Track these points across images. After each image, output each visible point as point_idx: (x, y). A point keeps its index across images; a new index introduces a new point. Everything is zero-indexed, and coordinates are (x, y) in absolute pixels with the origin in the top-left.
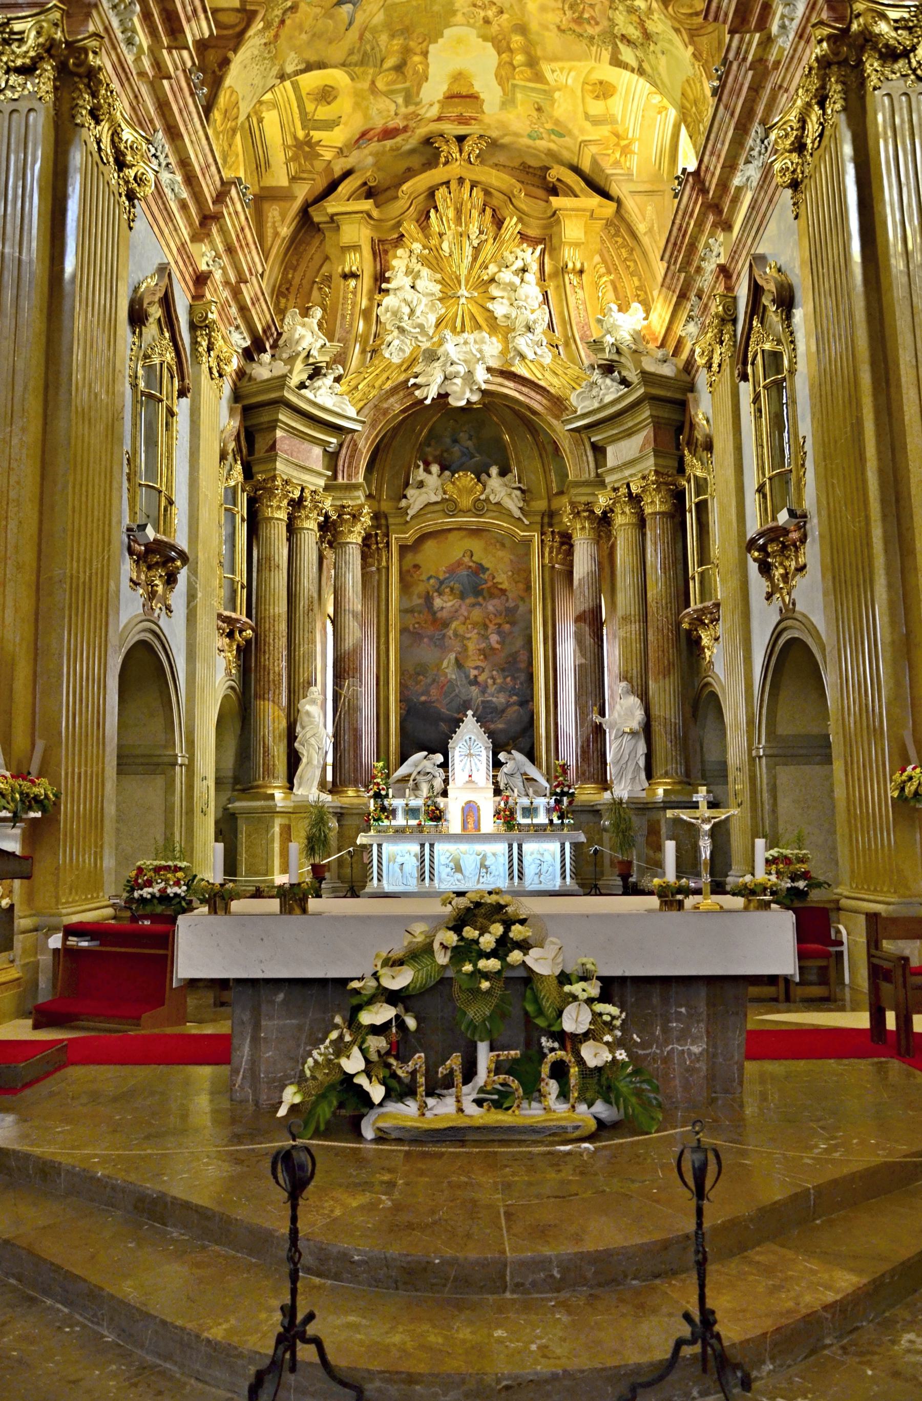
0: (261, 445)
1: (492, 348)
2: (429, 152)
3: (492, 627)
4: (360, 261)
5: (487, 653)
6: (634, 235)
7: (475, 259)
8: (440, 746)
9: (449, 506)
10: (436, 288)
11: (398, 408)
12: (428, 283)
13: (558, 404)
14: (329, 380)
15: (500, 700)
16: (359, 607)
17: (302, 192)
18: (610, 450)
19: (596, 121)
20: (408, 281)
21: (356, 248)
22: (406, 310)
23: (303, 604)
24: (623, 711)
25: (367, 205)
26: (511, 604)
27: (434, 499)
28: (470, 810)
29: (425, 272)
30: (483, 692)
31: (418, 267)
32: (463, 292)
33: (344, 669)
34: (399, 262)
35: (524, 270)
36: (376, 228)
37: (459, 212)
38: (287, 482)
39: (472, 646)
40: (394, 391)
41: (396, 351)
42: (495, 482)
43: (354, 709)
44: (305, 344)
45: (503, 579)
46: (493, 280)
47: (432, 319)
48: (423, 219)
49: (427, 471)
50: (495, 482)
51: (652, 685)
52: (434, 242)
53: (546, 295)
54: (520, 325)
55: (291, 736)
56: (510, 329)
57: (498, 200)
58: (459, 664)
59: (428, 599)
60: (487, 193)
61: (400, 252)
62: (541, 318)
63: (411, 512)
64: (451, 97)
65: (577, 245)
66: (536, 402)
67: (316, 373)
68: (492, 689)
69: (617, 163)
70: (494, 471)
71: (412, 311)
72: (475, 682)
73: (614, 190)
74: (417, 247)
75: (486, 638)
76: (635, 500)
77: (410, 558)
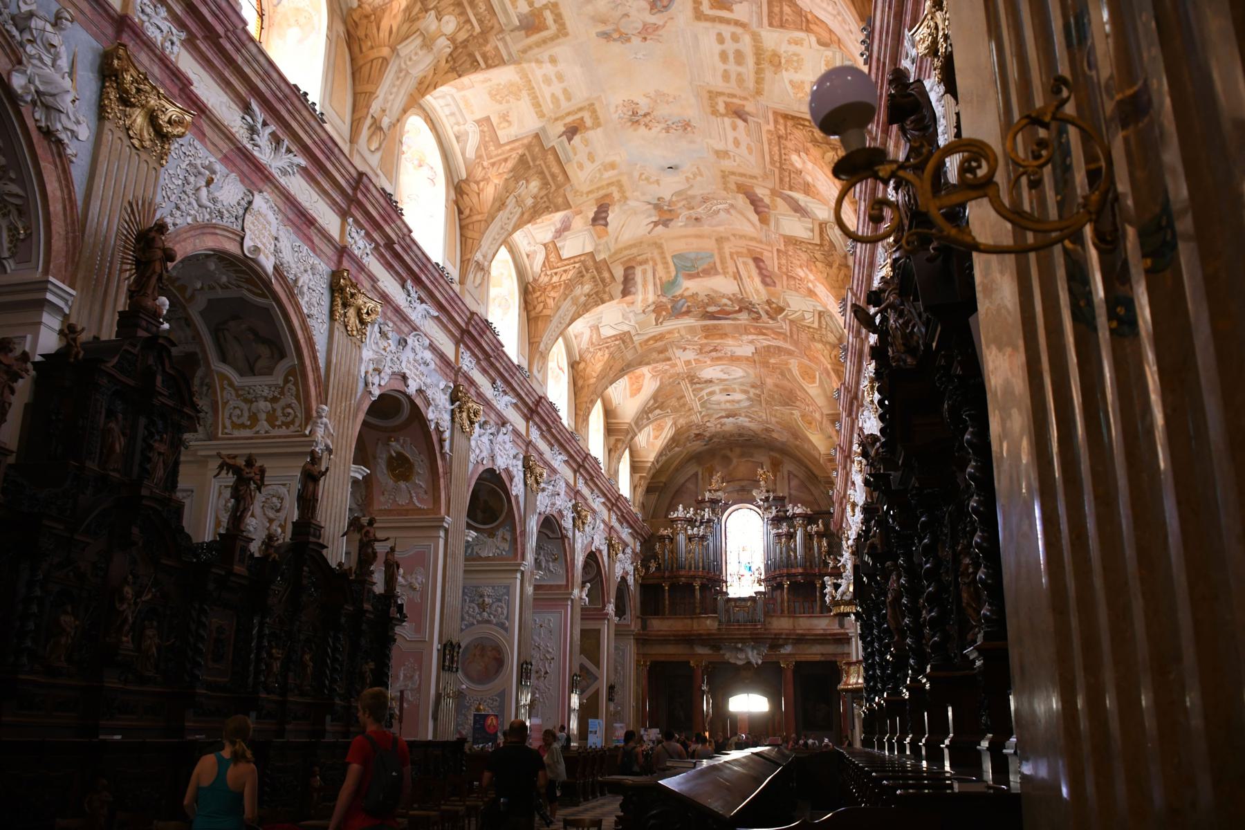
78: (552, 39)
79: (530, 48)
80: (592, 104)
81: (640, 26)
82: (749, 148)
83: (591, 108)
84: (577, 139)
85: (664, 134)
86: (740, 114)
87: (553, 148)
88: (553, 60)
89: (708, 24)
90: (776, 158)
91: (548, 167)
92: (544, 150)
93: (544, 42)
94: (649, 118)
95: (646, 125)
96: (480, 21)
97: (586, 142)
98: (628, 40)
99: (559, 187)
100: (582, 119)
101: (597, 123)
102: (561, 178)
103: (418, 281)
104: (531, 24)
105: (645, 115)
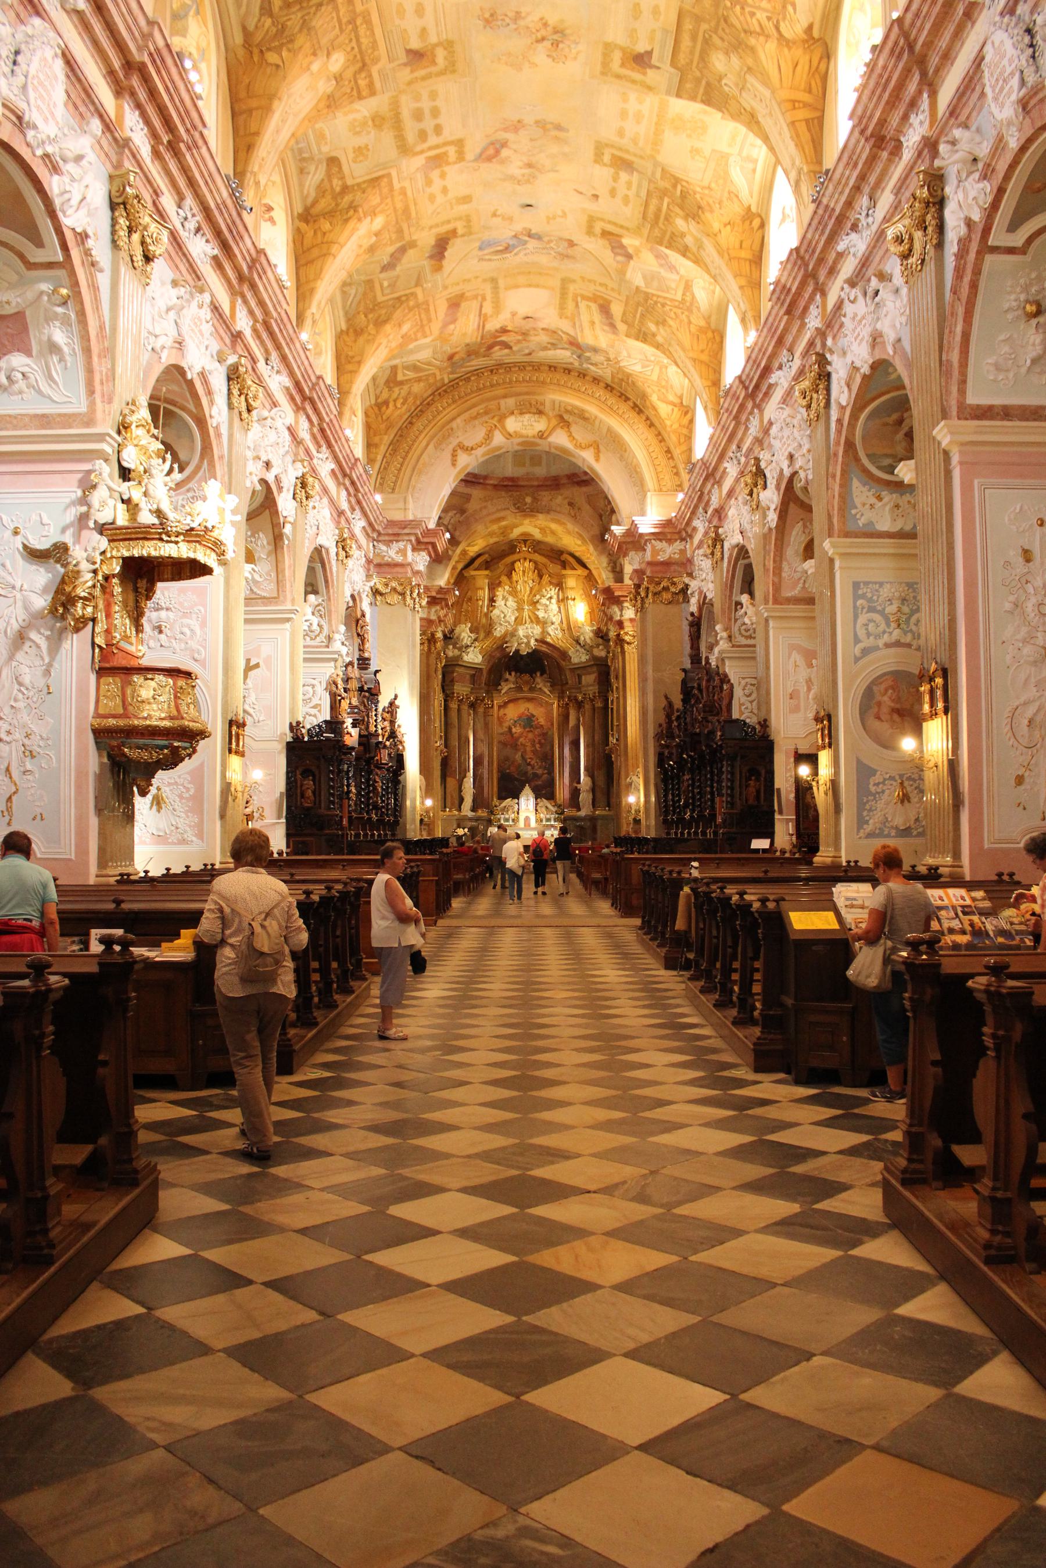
0: (448, 679)
1: (537, 630)
5: (534, 752)
8: (516, 796)
9: (519, 689)
10: (515, 605)
12: (511, 603)
13: (564, 655)
15: (540, 772)
21: (483, 589)
25: (487, 572)
28: (527, 819)
29: (510, 599)
34: (500, 593)
41: (498, 632)
43: (482, 778)
45: (542, 721)
48: (509, 576)
50: (538, 680)
55: (460, 791)
57: (540, 566)
59: (510, 729)
60: (536, 563)
62: (557, 620)
66: (555, 655)
67: (467, 647)
76: (592, 700)
77: (502, 712)
78: (612, 146)
79: (635, 155)
80: (603, 73)
81: (522, 132)
82: (401, 12)
83: (606, 70)
84: (641, 47)
85: (524, 10)
86: (416, 56)
87: (673, 63)
88: (621, 133)
89: (450, 139)
90: (362, 30)
91: (692, 53)
92: (683, 73)
93: (620, 149)
94: (539, 36)
95: (545, 25)
96: (661, 199)
97: (632, 33)
98: (537, 122)
99: (698, 19)
100: (623, 65)
101: (608, 48)
102: (688, 26)
103: (767, 371)
104: (623, 164)
105: (543, 39)
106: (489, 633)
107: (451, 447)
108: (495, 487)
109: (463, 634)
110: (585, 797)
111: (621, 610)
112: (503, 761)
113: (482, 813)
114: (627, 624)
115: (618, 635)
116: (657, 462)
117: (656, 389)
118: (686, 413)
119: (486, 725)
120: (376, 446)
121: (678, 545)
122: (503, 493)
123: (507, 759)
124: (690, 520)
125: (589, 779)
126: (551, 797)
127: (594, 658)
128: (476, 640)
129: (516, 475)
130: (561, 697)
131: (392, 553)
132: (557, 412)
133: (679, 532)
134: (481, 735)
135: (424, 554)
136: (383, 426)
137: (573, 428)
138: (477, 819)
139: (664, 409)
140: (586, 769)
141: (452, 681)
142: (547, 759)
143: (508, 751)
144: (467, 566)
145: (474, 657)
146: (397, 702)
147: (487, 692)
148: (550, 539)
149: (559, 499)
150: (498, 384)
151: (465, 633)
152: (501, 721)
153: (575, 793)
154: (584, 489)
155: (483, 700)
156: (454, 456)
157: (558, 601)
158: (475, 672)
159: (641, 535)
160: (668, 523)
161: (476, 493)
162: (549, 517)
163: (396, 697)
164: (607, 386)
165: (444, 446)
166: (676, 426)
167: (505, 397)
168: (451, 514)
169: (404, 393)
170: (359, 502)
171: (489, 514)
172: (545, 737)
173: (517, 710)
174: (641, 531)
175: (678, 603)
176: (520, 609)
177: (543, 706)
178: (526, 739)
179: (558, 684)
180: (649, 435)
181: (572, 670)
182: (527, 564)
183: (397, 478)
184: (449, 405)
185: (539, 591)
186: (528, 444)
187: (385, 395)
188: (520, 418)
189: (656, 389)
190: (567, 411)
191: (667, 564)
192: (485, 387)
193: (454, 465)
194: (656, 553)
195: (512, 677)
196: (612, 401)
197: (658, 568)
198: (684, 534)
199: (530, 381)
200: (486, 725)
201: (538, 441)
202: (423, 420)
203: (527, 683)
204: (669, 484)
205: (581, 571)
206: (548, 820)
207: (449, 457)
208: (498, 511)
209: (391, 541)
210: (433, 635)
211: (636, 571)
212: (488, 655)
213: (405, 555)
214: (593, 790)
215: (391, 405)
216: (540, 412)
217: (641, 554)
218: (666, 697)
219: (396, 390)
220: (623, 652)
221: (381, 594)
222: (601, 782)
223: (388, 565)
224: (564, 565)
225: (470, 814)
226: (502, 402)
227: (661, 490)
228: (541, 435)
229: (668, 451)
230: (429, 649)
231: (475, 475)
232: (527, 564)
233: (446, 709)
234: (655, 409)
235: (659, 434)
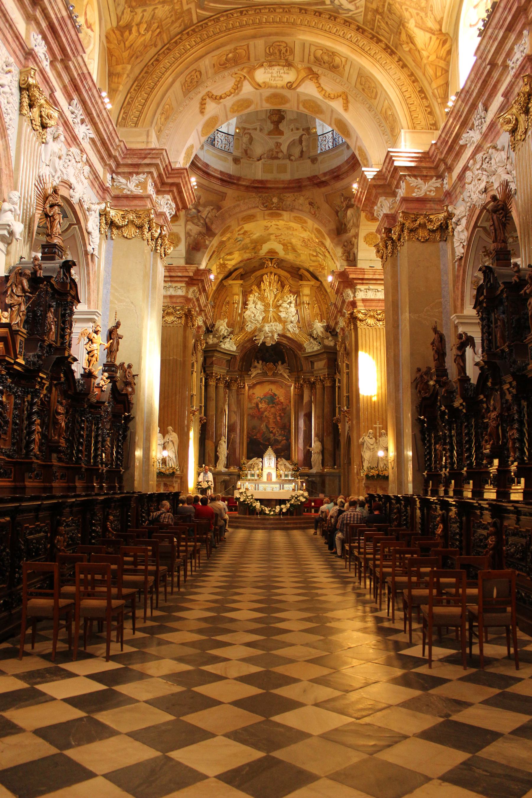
0: (208, 362)
1: (279, 327)
2: (262, 266)
3: (278, 414)
4: (238, 298)
5: (276, 423)
6: (326, 292)
7: (275, 299)
8: (260, 455)
9: (265, 374)
10: (262, 308)
11: (249, 346)
12: (260, 306)
13: (300, 347)
14: (228, 340)
15: (280, 438)
16: (236, 410)
17: (221, 277)
18: (315, 364)
19: (314, 261)
20: (253, 306)
22: (253, 315)
23: (219, 410)
24: (315, 445)
25: (241, 282)
26: (284, 407)
27: (260, 372)
28: (269, 475)
29: (259, 302)
30: (274, 435)
31: (257, 300)
32: (271, 309)
33: (231, 428)
35: (291, 303)
36: (243, 288)
37: (270, 283)
38: (216, 374)
39: (271, 421)
40: (248, 341)
41: (249, 328)
42: (280, 367)
43: (234, 442)
44: (223, 332)
45: (282, 399)
46: (280, 306)
47: (261, 318)
48: (259, 286)
49: (258, 363)
50: (280, 367)
51: (325, 439)
52: (263, 292)
53: (297, 311)
54: (289, 320)
55: (216, 451)
56: (285, 322)
57: (283, 279)
58: (267, 426)
59: (257, 405)
60: (279, 276)
61: (251, 295)
62: (295, 319)
63: (252, 376)
64: (268, 252)
65: (307, 295)
67: (224, 337)
68: (277, 435)
69: (320, 272)
70: (280, 363)
71: (255, 316)
72: (271, 432)
73: (320, 278)
74: (257, 294)
75: (275, 418)
76: (322, 381)
77: (251, 392)
106: (242, 329)
107: (200, 96)
108: (248, 188)
109: (221, 327)
110: (316, 458)
111: (354, 293)
112: (252, 430)
113: (233, 469)
114: (359, 304)
115: (352, 314)
116: (410, 101)
117: (414, 12)
118: (445, 42)
119: (239, 402)
120: (119, 75)
121: (434, 183)
122: (254, 195)
123: (254, 428)
124: (458, 136)
125: (319, 444)
126: (288, 458)
127: (325, 347)
128: (232, 333)
129: (264, 178)
130: (297, 380)
131: (131, 186)
132: (306, 65)
133: (437, 166)
134: (234, 408)
135: (168, 197)
136: (126, 54)
137: (323, 81)
138: (230, 474)
139: (421, 38)
140: (317, 435)
141: (212, 363)
142: (286, 428)
143: (255, 422)
144: (226, 277)
145: (230, 346)
146: (120, 331)
147: (241, 376)
148: (290, 257)
149: (301, 200)
150: (247, 24)
151: (222, 327)
152: (250, 398)
153: (308, 455)
154: (323, 189)
155: (236, 381)
156: (203, 104)
157: (296, 305)
158: (231, 358)
159: (396, 169)
160: (425, 157)
161: (230, 192)
162: (293, 214)
163: (118, 325)
164: (358, 28)
165: (192, 95)
166: (433, 57)
167: (254, 37)
168: (208, 209)
169: (147, 16)
170: (77, 88)
171: (241, 212)
172: (285, 412)
173: (263, 390)
174: (396, 164)
175: (434, 241)
176: (266, 311)
177: (284, 388)
178: (269, 413)
179: (295, 370)
180: (401, 75)
181: (307, 358)
182: (272, 277)
183: (141, 112)
184: (197, 44)
185: (282, 297)
186: (276, 97)
187: (127, 17)
188: (269, 70)
189: (414, 12)
190: (318, 61)
191: (422, 200)
192: (234, 28)
193: (202, 112)
194: (410, 189)
195: (259, 365)
196: (363, 42)
197: (411, 205)
198: (442, 167)
199: (281, 22)
200: (239, 402)
201: (287, 93)
202: (170, 58)
203: (270, 369)
204: (423, 123)
205: (313, 282)
206: (286, 476)
207: (198, 105)
208: (249, 209)
209: (131, 174)
210: (189, 311)
211: (386, 216)
212: (241, 346)
213: (145, 188)
214: (323, 452)
215: (134, 29)
216: (289, 65)
217: (391, 200)
218: (435, 330)
219: (139, 11)
220: (356, 328)
221: (118, 227)
222: (329, 446)
223: (127, 197)
224: (301, 278)
225: (224, 470)
226: (252, 43)
227: (415, 128)
228: (290, 86)
229: (422, 91)
230: (186, 324)
231: (229, 176)
232: (272, 277)
233: (206, 385)
234: (411, 39)
235: (412, 74)
